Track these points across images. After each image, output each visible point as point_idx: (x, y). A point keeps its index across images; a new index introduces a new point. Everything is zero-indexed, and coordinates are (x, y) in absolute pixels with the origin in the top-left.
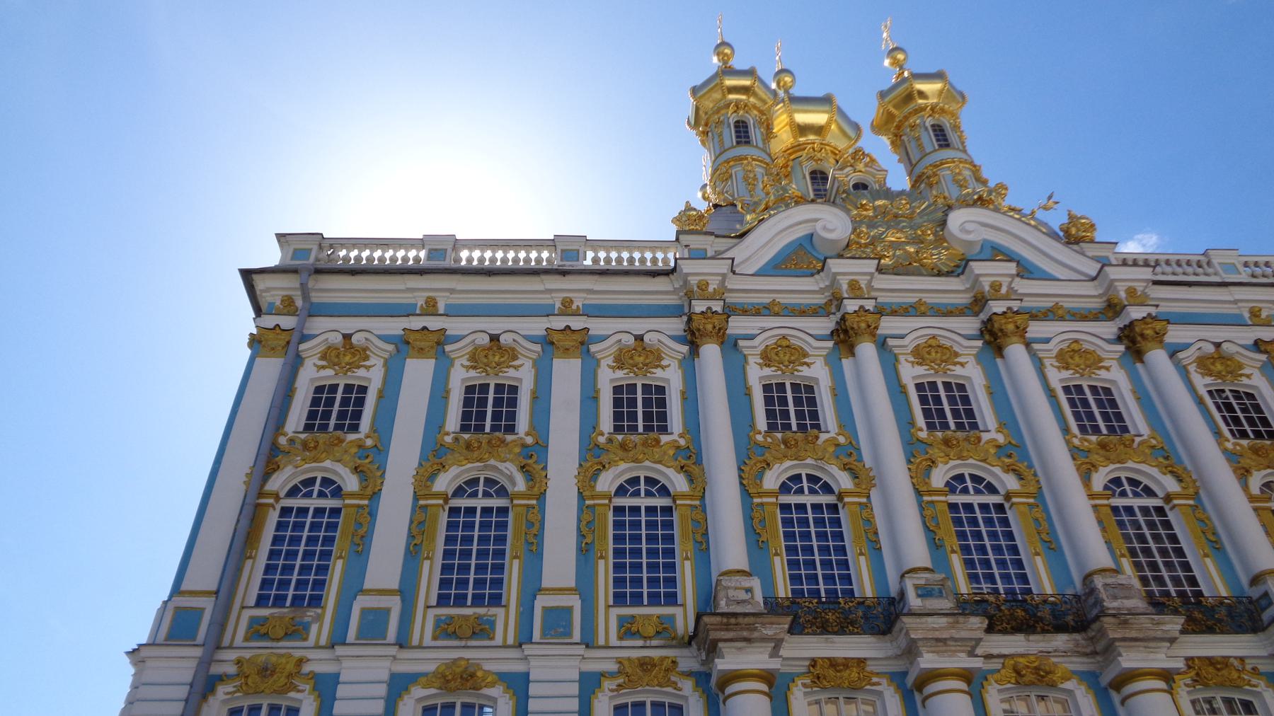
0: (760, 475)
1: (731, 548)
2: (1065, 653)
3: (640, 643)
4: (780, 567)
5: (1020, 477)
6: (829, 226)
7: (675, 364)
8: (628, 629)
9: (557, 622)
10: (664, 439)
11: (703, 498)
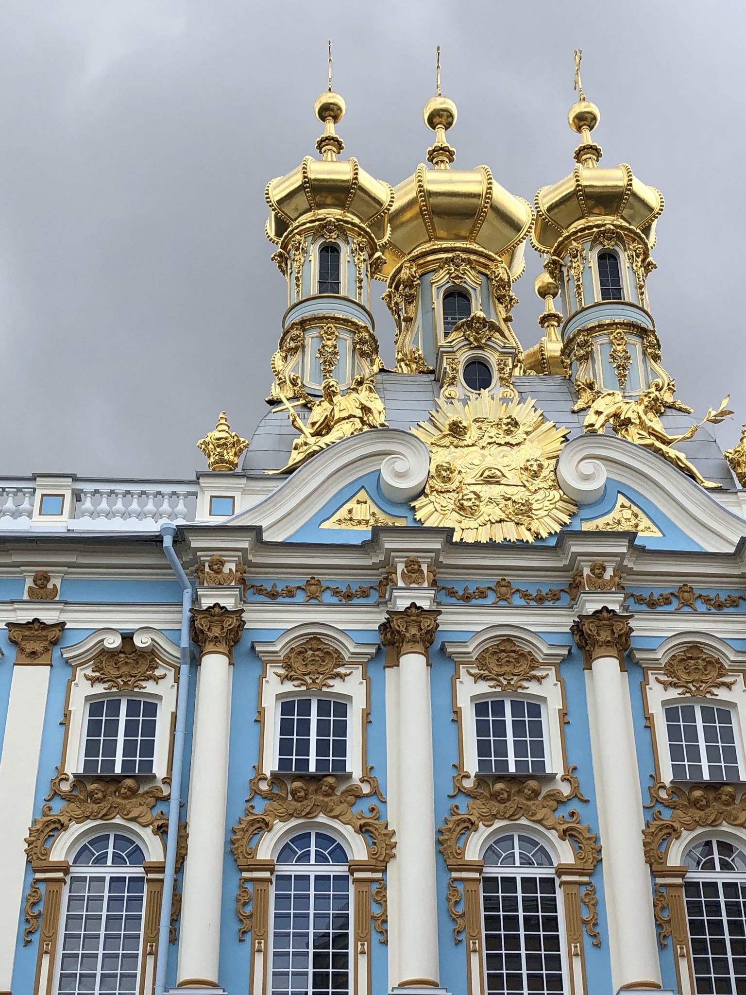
6: (400, 466)
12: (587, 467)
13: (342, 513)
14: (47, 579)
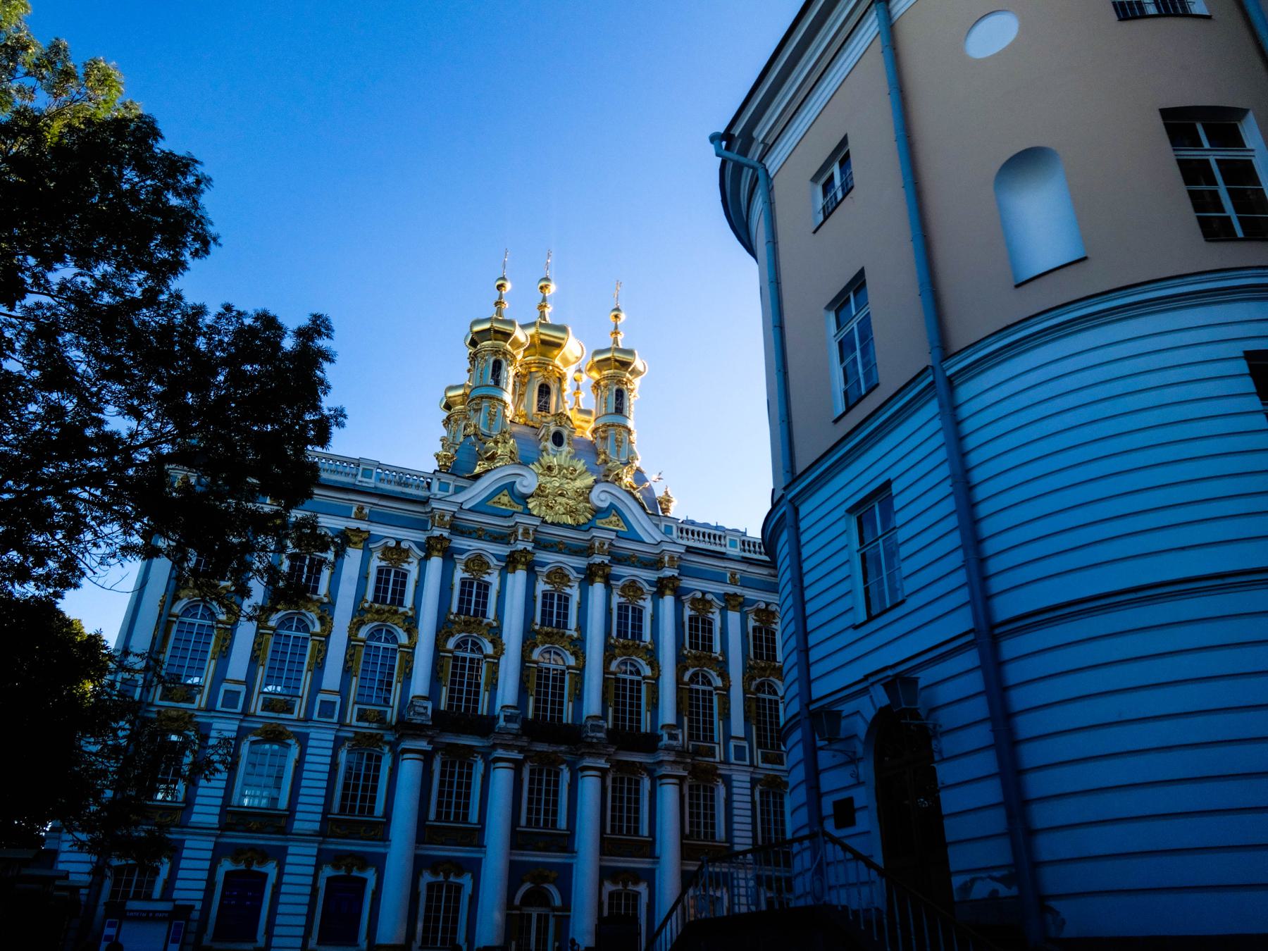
0: (446, 640)
1: (420, 684)
2: (565, 753)
3: (366, 724)
4: (444, 692)
5: (577, 658)
6: (525, 483)
7: (416, 562)
8: (362, 716)
9: (327, 708)
10: (401, 610)
11: (414, 648)
12: (603, 496)
13: (496, 499)
14: (362, 508)
